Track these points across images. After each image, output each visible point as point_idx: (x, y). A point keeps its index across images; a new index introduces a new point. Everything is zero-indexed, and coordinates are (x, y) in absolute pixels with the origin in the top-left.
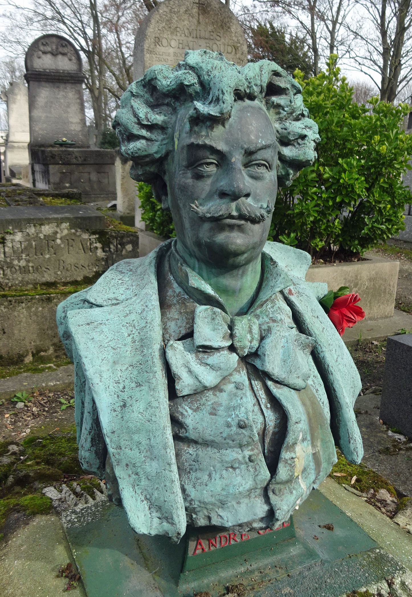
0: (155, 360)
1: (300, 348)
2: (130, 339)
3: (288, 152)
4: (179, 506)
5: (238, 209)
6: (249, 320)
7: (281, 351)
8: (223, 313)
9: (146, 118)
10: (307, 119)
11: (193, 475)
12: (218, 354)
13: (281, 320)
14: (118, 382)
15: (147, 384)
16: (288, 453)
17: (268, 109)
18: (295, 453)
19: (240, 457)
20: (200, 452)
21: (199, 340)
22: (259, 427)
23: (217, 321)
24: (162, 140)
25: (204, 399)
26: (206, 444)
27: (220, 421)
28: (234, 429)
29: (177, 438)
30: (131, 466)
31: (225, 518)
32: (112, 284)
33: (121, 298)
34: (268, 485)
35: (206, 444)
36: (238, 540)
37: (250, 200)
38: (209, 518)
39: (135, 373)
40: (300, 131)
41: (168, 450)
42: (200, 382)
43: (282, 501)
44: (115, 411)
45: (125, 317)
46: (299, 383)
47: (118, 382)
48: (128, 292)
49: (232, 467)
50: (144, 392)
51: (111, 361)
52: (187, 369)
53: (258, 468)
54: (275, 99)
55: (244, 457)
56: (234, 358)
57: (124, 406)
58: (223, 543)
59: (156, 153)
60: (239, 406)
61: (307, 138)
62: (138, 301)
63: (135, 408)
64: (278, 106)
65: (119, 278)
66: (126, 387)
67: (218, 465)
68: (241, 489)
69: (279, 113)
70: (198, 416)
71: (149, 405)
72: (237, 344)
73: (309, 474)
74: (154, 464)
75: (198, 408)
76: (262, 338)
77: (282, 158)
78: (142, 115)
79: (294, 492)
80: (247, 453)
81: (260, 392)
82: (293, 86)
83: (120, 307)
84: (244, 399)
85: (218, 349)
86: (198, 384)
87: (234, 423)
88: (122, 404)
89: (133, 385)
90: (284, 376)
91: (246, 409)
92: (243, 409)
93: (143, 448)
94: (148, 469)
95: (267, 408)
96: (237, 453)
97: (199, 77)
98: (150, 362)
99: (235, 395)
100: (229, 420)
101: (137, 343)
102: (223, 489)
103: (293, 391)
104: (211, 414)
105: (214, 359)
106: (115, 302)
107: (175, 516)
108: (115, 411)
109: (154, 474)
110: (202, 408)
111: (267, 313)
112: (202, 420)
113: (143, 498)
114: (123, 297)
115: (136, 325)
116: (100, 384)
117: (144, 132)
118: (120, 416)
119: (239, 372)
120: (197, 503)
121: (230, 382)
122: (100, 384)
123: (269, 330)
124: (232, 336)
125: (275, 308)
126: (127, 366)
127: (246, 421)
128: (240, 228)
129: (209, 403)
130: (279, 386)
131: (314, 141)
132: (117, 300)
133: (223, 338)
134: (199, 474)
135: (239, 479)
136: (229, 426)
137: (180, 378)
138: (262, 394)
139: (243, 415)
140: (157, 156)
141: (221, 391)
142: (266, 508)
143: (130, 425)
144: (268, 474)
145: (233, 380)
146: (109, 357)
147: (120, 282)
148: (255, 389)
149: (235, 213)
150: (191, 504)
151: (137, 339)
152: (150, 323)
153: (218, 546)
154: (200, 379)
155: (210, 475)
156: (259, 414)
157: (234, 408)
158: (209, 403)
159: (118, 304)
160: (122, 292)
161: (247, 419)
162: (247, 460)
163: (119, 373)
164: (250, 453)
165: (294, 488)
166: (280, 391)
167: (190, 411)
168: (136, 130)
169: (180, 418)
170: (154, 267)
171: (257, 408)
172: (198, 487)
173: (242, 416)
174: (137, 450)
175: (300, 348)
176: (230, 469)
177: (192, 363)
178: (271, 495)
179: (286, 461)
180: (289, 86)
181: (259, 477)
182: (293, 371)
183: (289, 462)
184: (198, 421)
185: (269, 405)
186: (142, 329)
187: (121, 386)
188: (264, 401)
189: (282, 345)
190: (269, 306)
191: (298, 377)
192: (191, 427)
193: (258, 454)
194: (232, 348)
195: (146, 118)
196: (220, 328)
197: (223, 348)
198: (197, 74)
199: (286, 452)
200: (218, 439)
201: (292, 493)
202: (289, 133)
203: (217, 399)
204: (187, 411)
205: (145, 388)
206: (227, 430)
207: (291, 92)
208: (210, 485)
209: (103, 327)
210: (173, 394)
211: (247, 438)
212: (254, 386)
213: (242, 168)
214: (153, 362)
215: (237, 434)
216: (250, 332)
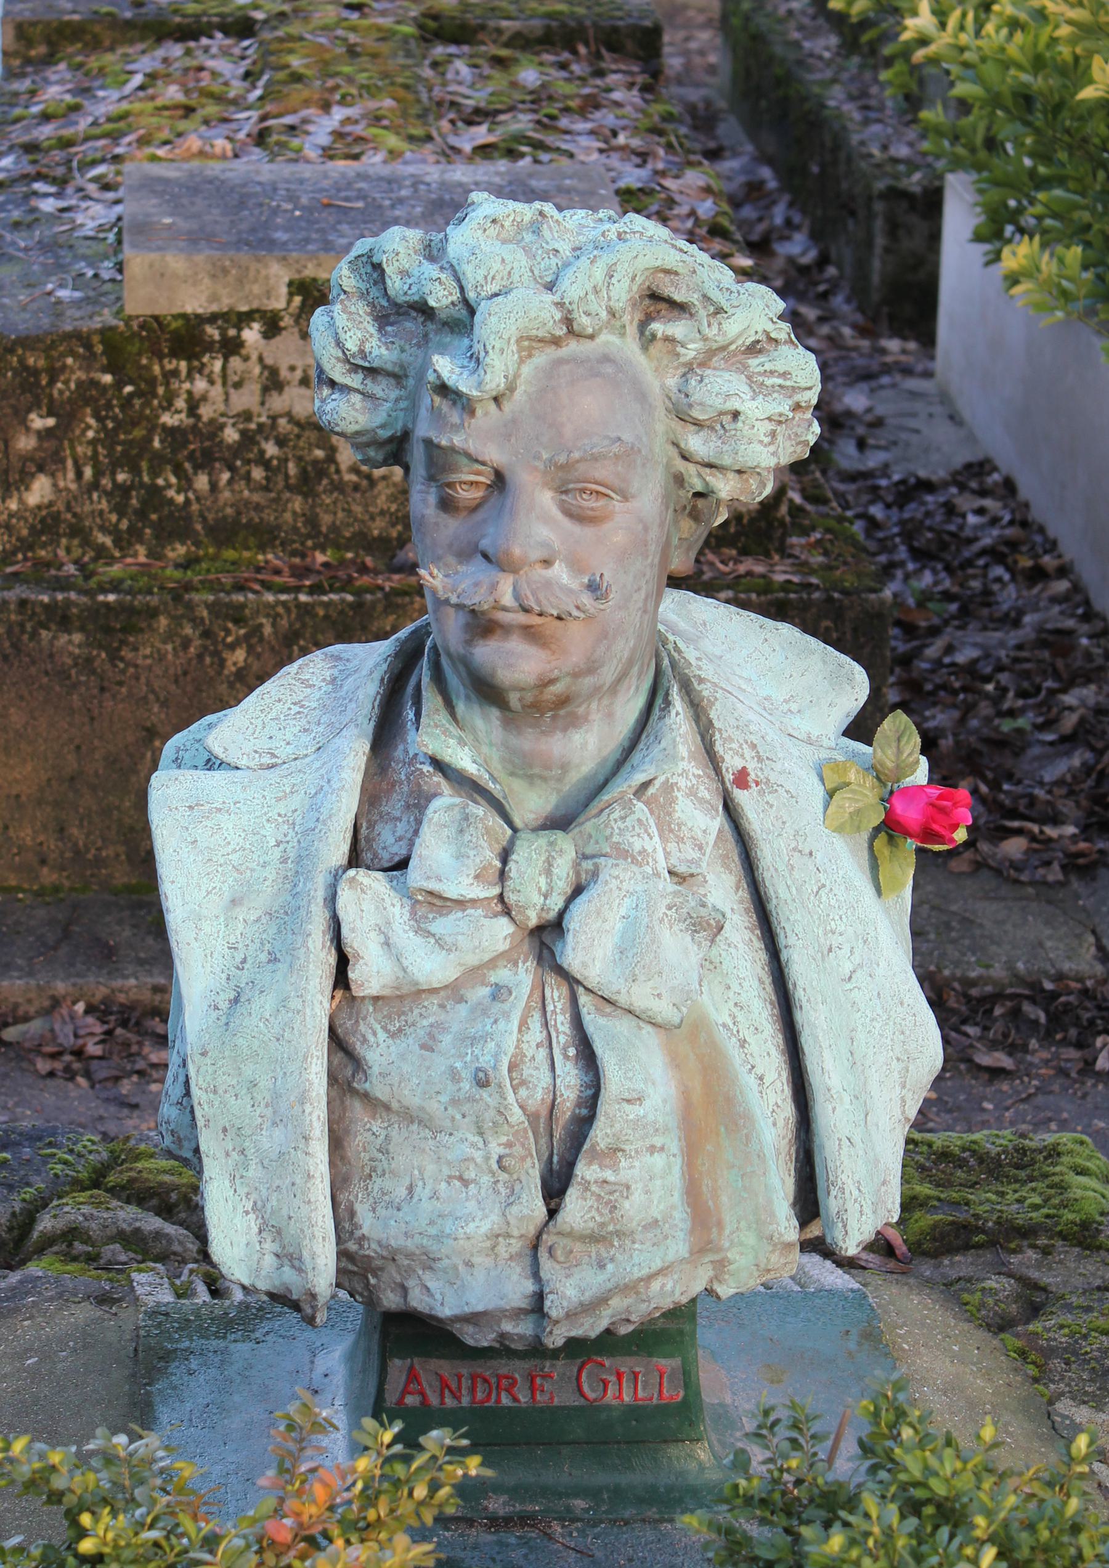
0: (313, 908)
1: (683, 926)
2: (277, 853)
3: (697, 443)
4: (319, 1235)
5: (517, 596)
6: (551, 844)
7: (619, 926)
9: (362, 351)
10: (785, 349)
11: (377, 1184)
12: (460, 914)
13: (643, 852)
14: (233, 948)
15: (289, 958)
16: (595, 1167)
17: (645, 348)
18: (616, 1170)
19: (478, 1156)
20: (394, 1133)
22: (539, 1095)
23: (467, 837)
24: (397, 400)
25: (416, 1012)
26: (409, 1116)
28: (466, 1086)
30: (231, 1133)
31: (438, 1297)
32: (273, 714)
34: (539, 1236)
36: (523, 1399)
38: (404, 1290)
39: (273, 930)
40: (718, 403)
41: (308, 1108)
42: (404, 970)
43: (568, 1276)
44: (216, 1008)
45: (278, 799)
46: (664, 1010)
47: (233, 948)
48: (305, 739)
49: (461, 1178)
50: (279, 976)
51: (227, 896)
52: (382, 939)
53: (517, 1187)
55: (487, 1158)
56: (503, 927)
57: (236, 1000)
58: (480, 1395)
59: (383, 426)
60: (485, 1038)
61: (741, 418)
62: (317, 764)
63: (255, 1006)
64: (669, 340)
65: (296, 699)
66: (250, 961)
68: (471, 1228)
69: (678, 355)
70: (396, 1048)
71: (284, 1002)
72: (511, 898)
73: (666, 1237)
74: (278, 1133)
75: (400, 1030)
76: (578, 891)
78: (352, 345)
79: (610, 1267)
81: (560, 1018)
82: (706, 298)
83: (273, 775)
84: (502, 1025)
85: (461, 904)
86: (401, 974)
87: (466, 1074)
88: (232, 995)
89: (264, 957)
90: (615, 988)
91: (498, 1046)
92: (491, 1045)
93: (259, 1097)
94: (265, 1144)
95: (566, 1057)
96: (473, 1145)
97: (462, 289)
98: (303, 912)
99: (485, 1012)
100: (458, 1065)
101: (290, 865)
102: (432, 1223)
103: (649, 1028)
104: (423, 1047)
106: (267, 760)
107: (306, 1254)
108: (216, 1008)
109: (274, 1157)
110: (408, 1031)
111: (608, 832)
112: (402, 1056)
113: (249, 1206)
114: (289, 749)
115: (298, 821)
116: (195, 945)
117: (354, 380)
118: (224, 1019)
119: (516, 964)
120: (374, 1246)
121: (484, 984)
122: (195, 945)
123: (595, 874)
124: (502, 875)
125: (629, 822)
126: (259, 913)
127: (491, 1073)
129: (425, 1023)
130: (608, 1009)
131: (769, 419)
132: (273, 755)
133: (477, 877)
134: (387, 1183)
135: (472, 1205)
136: (454, 1076)
137: (358, 956)
138: (562, 1023)
139: (487, 1058)
140: (384, 434)
141: (461, 1000)
142: (530, 1287)
143: (241, 1041)
144: (540, 1209)
145: (493, 980)
146: (225, 887)
147: (296, 709)
148: (550, 1008)
150: (361, 1247)
151: (292, 855)
152: (324, 823)
153: (465, 1401)
154: (405, 963)
155: (411, 1189)
156: (545, 1068)
157: (474, 1040)
158: (425, 1023)
159: (273, 766)
160: (289, 737)
161: (495, 1068)
162: (495, 1166)
163: (241, 926)
164: (501, 1150)
165: (612, 1260)
166: (602, 1021)
167: (382, 1035)
168: (338, 373)
169: (358, 1045)
170: (377, 683)
171: (543, 1053)
172: (381, 1211)
173: (486, 1060)
174: (248, 1099)
175: (683, 926)
176: (457, 1183)
177: (396, 926)
179: (586, 1185)
180: (694, 298)
181: (515, 1209)
182: (642, 978)
183: (594, 1188)
184: (393, 1057)
185: (572, 1052)
186: (305, 833)
187: (239, 957)
188: (562, 1039)
189: (623, 912)
190: (616, 815)
191: (659, 995)
192: (376, 1070)
193: (523, 1159)
195: (362, 351)
196: (472, 853)
197: (473, 901)
198: (458, 281)
199: (590, 1163)
200: (434, 1107)
201: (602, 1266)
202: (690, 406)
203: (443, 1017)
204: (375, 1034)
205: (282, 967)
206: (451, 1087)
208: (405, 1208)
209: (222, 818)
211: (492, 1113)
212: (548, 1000)
214: (309, 912)
215: (471, 1099)
216: (548, 872)
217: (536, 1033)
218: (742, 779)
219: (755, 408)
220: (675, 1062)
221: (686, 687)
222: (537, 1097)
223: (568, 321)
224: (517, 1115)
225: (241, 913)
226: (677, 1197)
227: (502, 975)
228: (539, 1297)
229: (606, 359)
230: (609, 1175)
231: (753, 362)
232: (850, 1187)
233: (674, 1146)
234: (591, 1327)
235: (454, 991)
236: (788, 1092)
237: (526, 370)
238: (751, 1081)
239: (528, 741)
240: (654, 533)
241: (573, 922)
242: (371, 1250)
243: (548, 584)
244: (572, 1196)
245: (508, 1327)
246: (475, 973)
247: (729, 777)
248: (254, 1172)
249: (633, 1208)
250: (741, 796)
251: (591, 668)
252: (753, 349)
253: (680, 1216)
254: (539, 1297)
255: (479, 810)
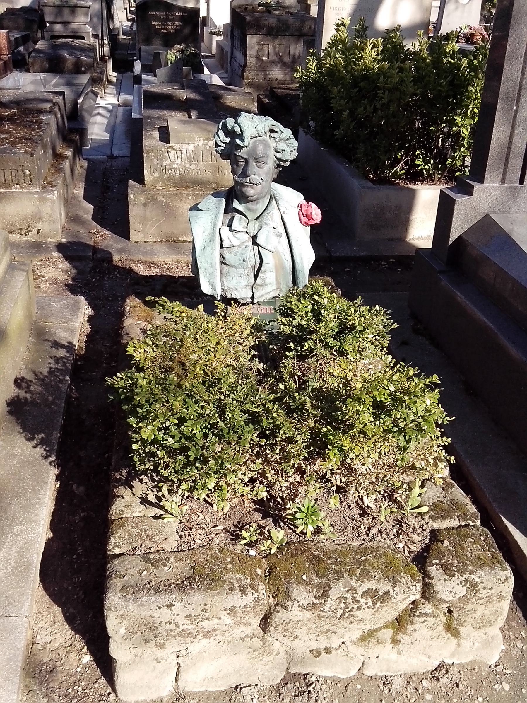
3: (278, 155)
8: (245, 218)
11: (227, 277)
21: (233, 228)
26: (232, 266)
27: (237, 258)
28: (242, 261)
29: (222, 262)
33: (211, 208)
35: (232, 266)
37: (256, 176)
46: (273, 250)
54: (273, 135)
60: (245, 253)
67: (236, 275)
68: (242, 284)
77: (276, 157)
80: (246, 272)
87: (242, 260)
99: (244, 250)
105: (238, 235)
124: (247, 228)
128: (252, 187)
134: (229, 277)
135: (242, 281)
136: (240, 260)
149: (248, 181)
173: (244, 258)
178: (254, 288)
180: (278, 130)
194: (247, 232)
200: (236, 265)
207: (280, 132)
210: (222, 247)
213: (254, 164)
217: (253, 253)
218: (284, 213)
219: (288, 149)
220: (274, 258)
221: (275, 197)
222: (253, 263)
223: (258, 134)
224: (250, 266)
225: (204, 234)
226: (274, 280)
227: (247, 244)
228: (253, 295)
229: (264, 140)
230: (264, 275)
231: (287, 142)
232: (301, 278)
233: (274, 271)
234: (261, 300)
235: (239, 246)
236: (291, 263)
237: (251, 142)
238: (286, 261)
239: (250, 205)
240: (271, 171)
241: (258, 235)
242: (226, 288)
243: (255, 179)
244: (258, 278)
245: (248, 300)
246: (243, 243)
247: (282, 213)
248: (208, 275)
249: (268, 281)
250: (283, 215)
251: (261, 193)
252: (287, 140)
253: (275, 283)
254: (253, 295)
255: (243, 217)
